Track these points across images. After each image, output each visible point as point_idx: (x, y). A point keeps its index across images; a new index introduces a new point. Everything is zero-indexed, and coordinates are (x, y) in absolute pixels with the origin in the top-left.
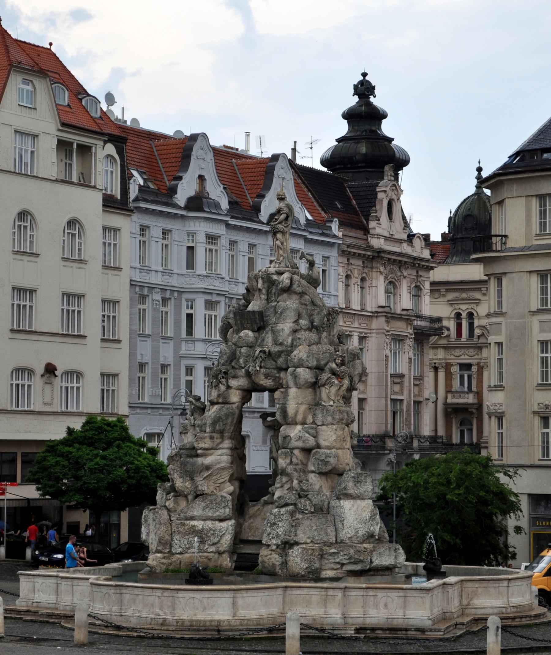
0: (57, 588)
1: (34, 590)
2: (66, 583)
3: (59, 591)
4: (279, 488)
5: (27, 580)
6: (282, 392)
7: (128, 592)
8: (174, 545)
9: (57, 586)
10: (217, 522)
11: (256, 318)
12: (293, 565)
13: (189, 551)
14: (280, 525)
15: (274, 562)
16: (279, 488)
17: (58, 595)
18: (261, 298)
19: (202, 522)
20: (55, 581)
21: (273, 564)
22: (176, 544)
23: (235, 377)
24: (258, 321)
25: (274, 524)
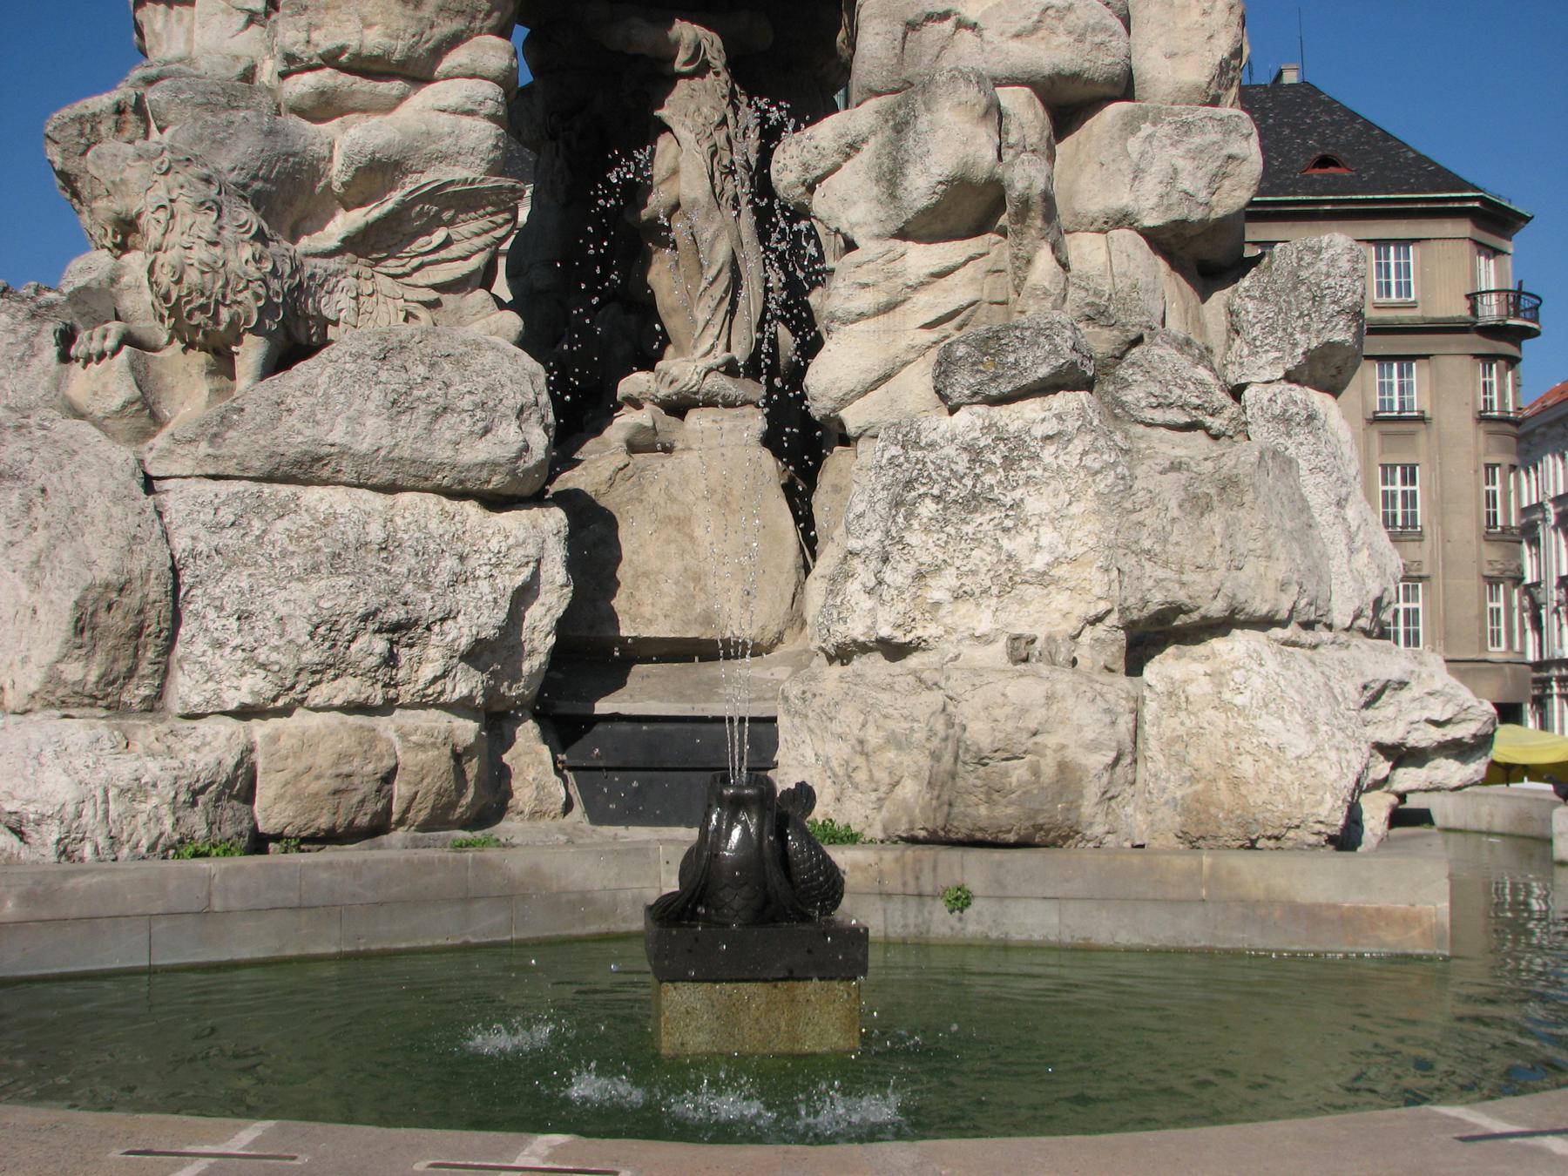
4: (861, 316)
10: (471, 508)
12: (1246, 767)
13: (318, 696)
14: (1035, 504)
15: (1075, 754)
16: (861, 316)
19: (378, 501)
21: (1063, 767)
22: (219, 644)
25: (974, 502)
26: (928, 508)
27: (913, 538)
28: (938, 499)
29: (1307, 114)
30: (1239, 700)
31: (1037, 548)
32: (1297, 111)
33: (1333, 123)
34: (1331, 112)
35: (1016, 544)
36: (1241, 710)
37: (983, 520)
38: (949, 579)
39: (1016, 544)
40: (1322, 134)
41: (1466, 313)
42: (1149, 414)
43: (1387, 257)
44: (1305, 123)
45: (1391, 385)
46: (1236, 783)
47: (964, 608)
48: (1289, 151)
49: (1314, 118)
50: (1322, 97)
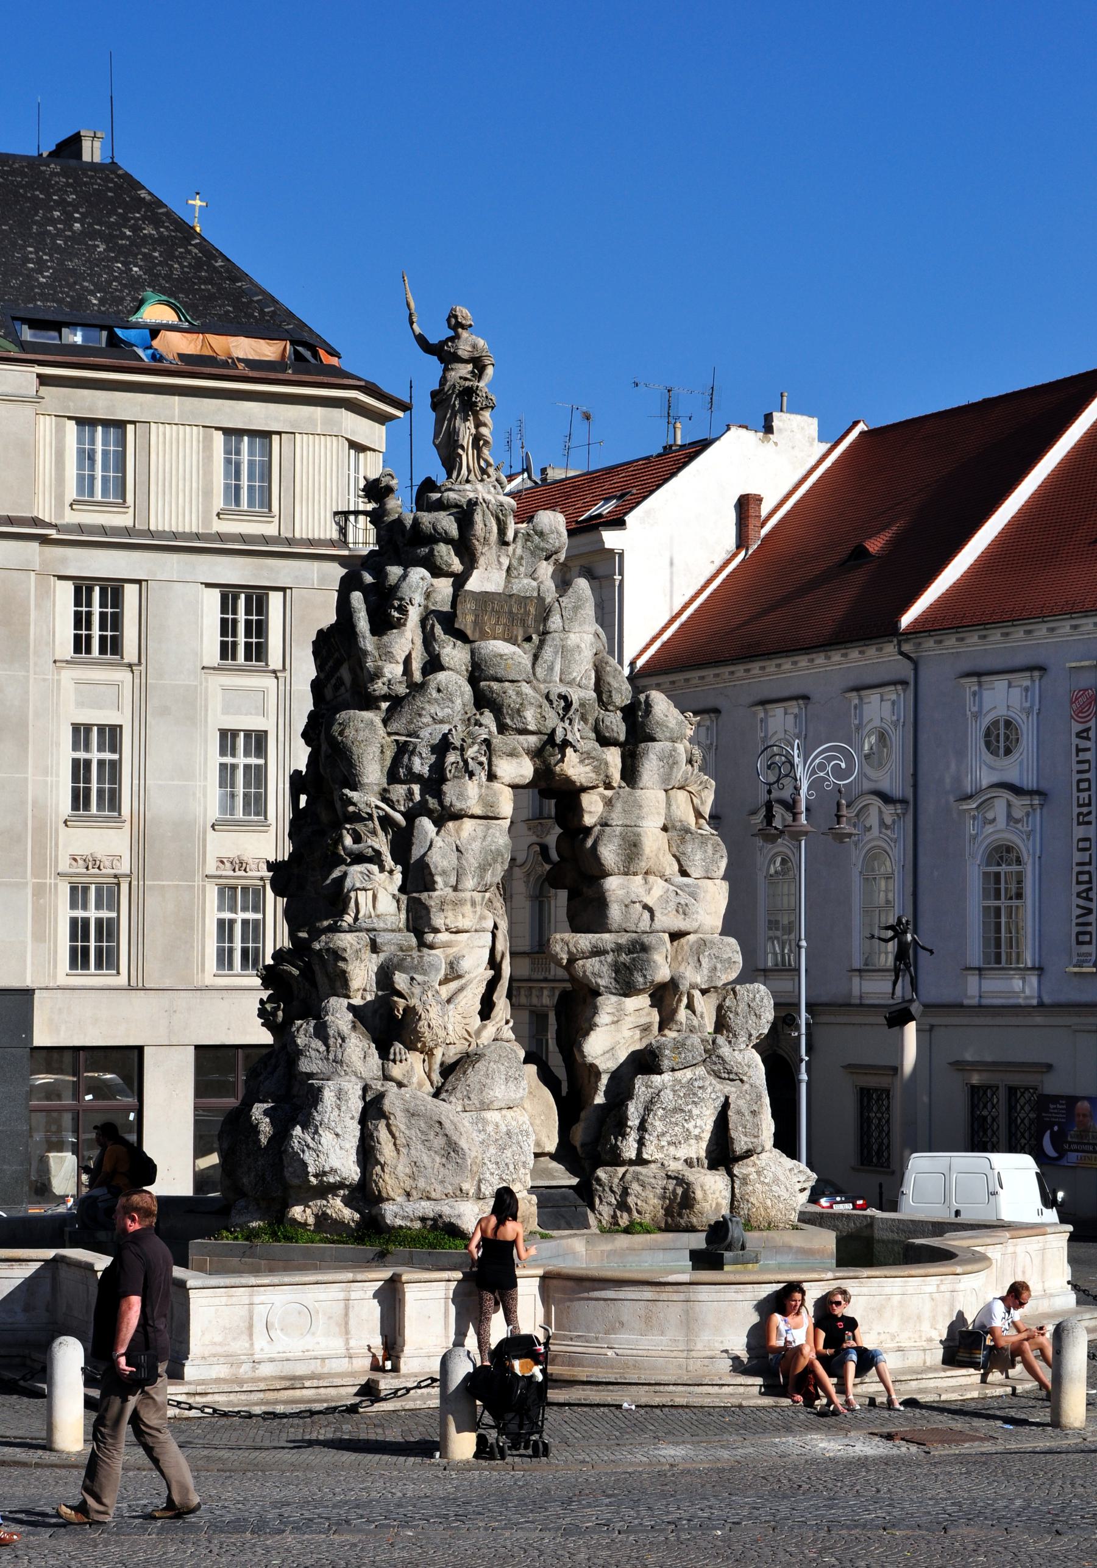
0: (346, 1315)
1: (251, 1327)
2: (420, 1295)
3: (352, 1322)
5: (224, 1300)
6: (603, 797)
7: (865, 1290)
8: (488, 1175)
9: (347, 1308)
11: (527, 613)
12: (769, 1203)
14: (695, 1111)
17: (347, 1332)
18: (499, 563)
20: (342, 1296)
22: (492, 1174)
23: (512, 754)
24: (530, 621)
26: (660, 1112)
27: (657, 1123)
28: (664, 1109)
29: (124, 220)
30: (766, 1181)
31: (696, 1127)
32: (109, 215)
33: (161, 240)
34: (157, 222)
35: (690, 1126)
36: (767, 1184)
37: (679, 1117)
38: (668, 1138)
39: (690, 1126)
40: (147, 257)
41: (335, 535)
42: (723, 1075)
43: (238, 452)
44: (123, 236)
45: (248, 634)
46: (766, 1209)
47: (672, 1148)
48: (109, 283)
49: (136, 229)
50: (143, 194)
